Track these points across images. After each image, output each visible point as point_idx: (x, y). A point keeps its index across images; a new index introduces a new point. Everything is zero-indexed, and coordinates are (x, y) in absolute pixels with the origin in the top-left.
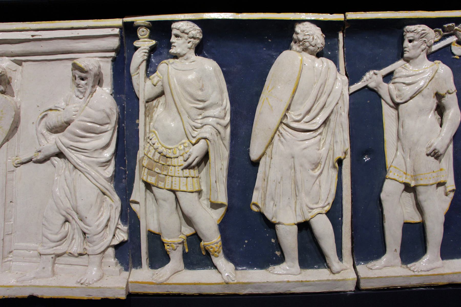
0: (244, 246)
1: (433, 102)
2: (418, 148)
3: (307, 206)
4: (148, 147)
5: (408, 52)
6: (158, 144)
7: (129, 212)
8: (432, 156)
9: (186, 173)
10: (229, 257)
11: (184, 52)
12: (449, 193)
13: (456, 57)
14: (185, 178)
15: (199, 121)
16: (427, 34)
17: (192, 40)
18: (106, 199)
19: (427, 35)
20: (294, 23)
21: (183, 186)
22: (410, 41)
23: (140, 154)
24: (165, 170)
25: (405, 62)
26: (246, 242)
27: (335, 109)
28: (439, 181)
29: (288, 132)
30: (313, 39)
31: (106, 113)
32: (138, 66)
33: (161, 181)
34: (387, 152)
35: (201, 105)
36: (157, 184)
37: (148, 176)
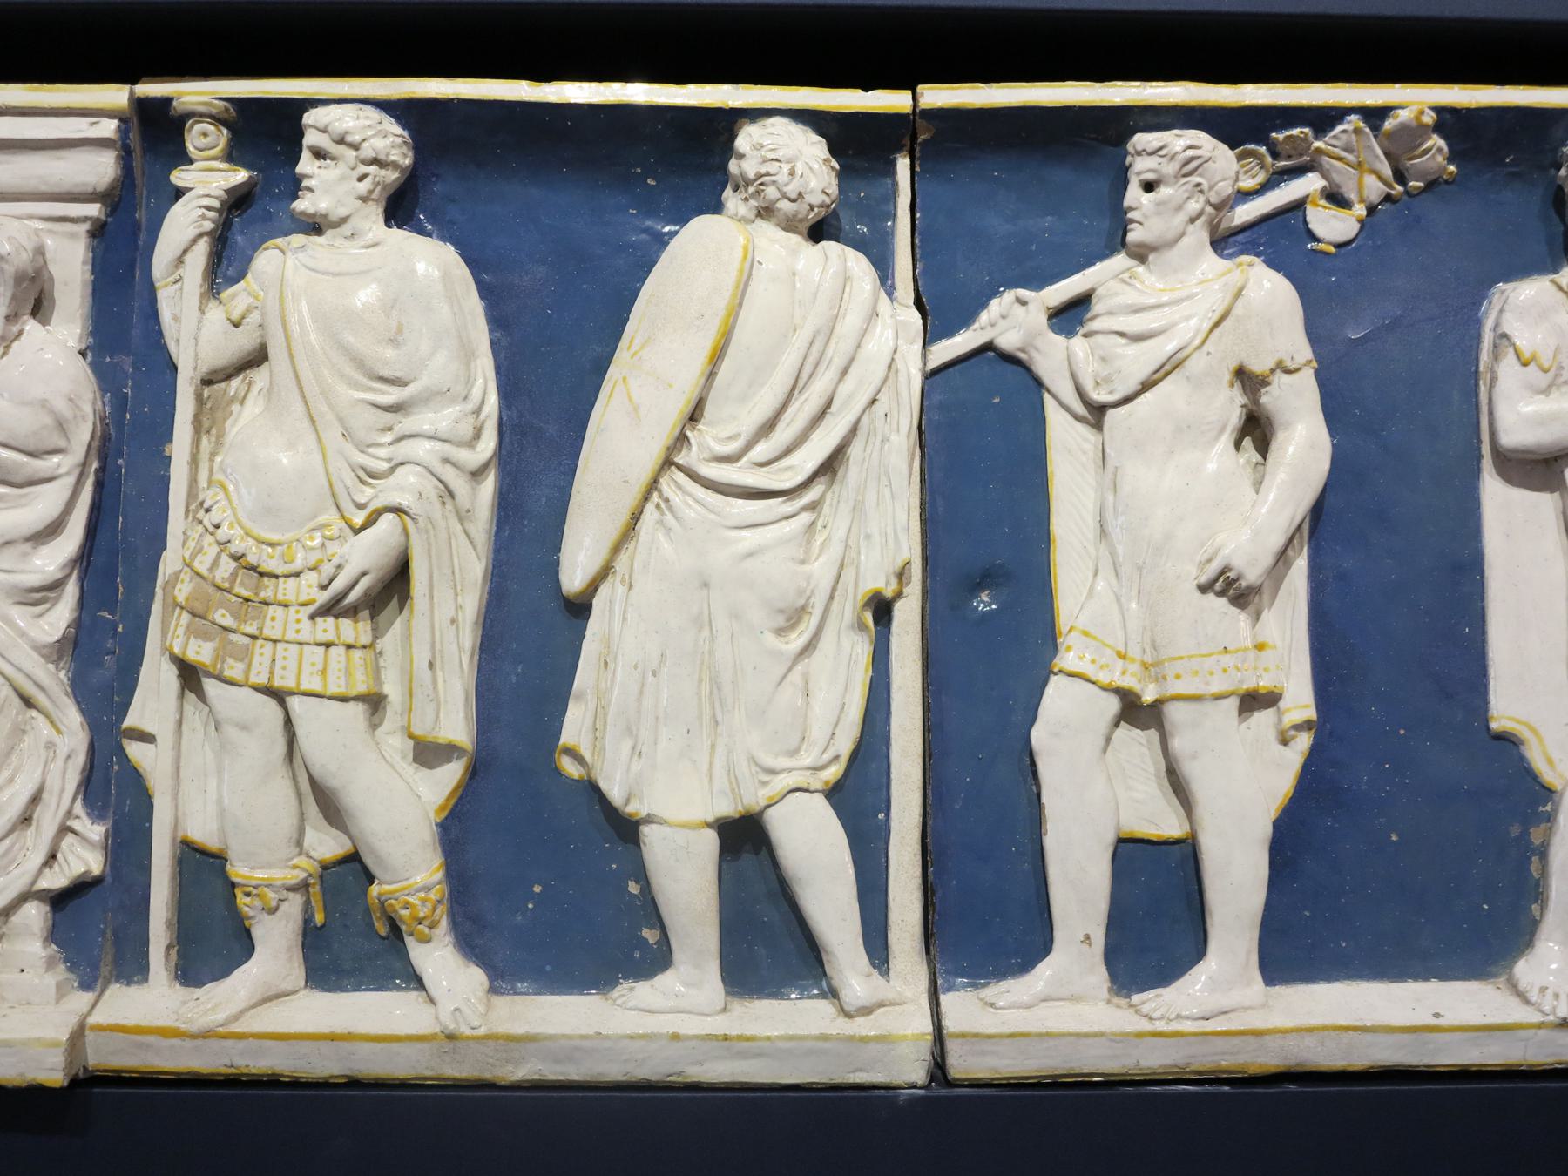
0: (530, 906)
1: (1230, 406)
2: (1169, 564)
3: (753, 760)
4: (197, 536)
5: (1140, 223)
6: (231, 526)
7: (117, 772)
8: (1221, 594)
9: (325, 631)
10: (471, 944)
11: (342, 212)
12: (1293, 733)
13: (1321, 246)
14: (322, 649)
15: (382, 452)
16: (1206, 162)
17: (373, 169)
18: (33, 721)
19: (1205, 165)
20: (731, 120)
21: (312, 674)
22: (1149, 187)
23: (169, 563)
24: (253, 619)
25: (1132, 262)
27: (865, 420)
28: (1248, 685)
29: (690, 495)
30: (792, 173)
31: (52, 412)
32: (179, 253)
33: (236, 659)
34: (1059, 580)
35: (391, 395)
36: (219, 666)
37: (188, 638)
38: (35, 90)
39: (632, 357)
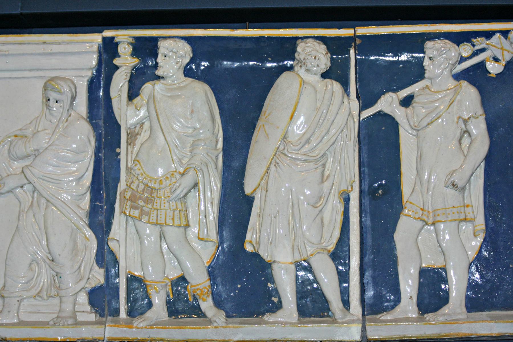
21: (170, 219)
26: (239, 286)
38: (72, 36)
39: (266, 118)
